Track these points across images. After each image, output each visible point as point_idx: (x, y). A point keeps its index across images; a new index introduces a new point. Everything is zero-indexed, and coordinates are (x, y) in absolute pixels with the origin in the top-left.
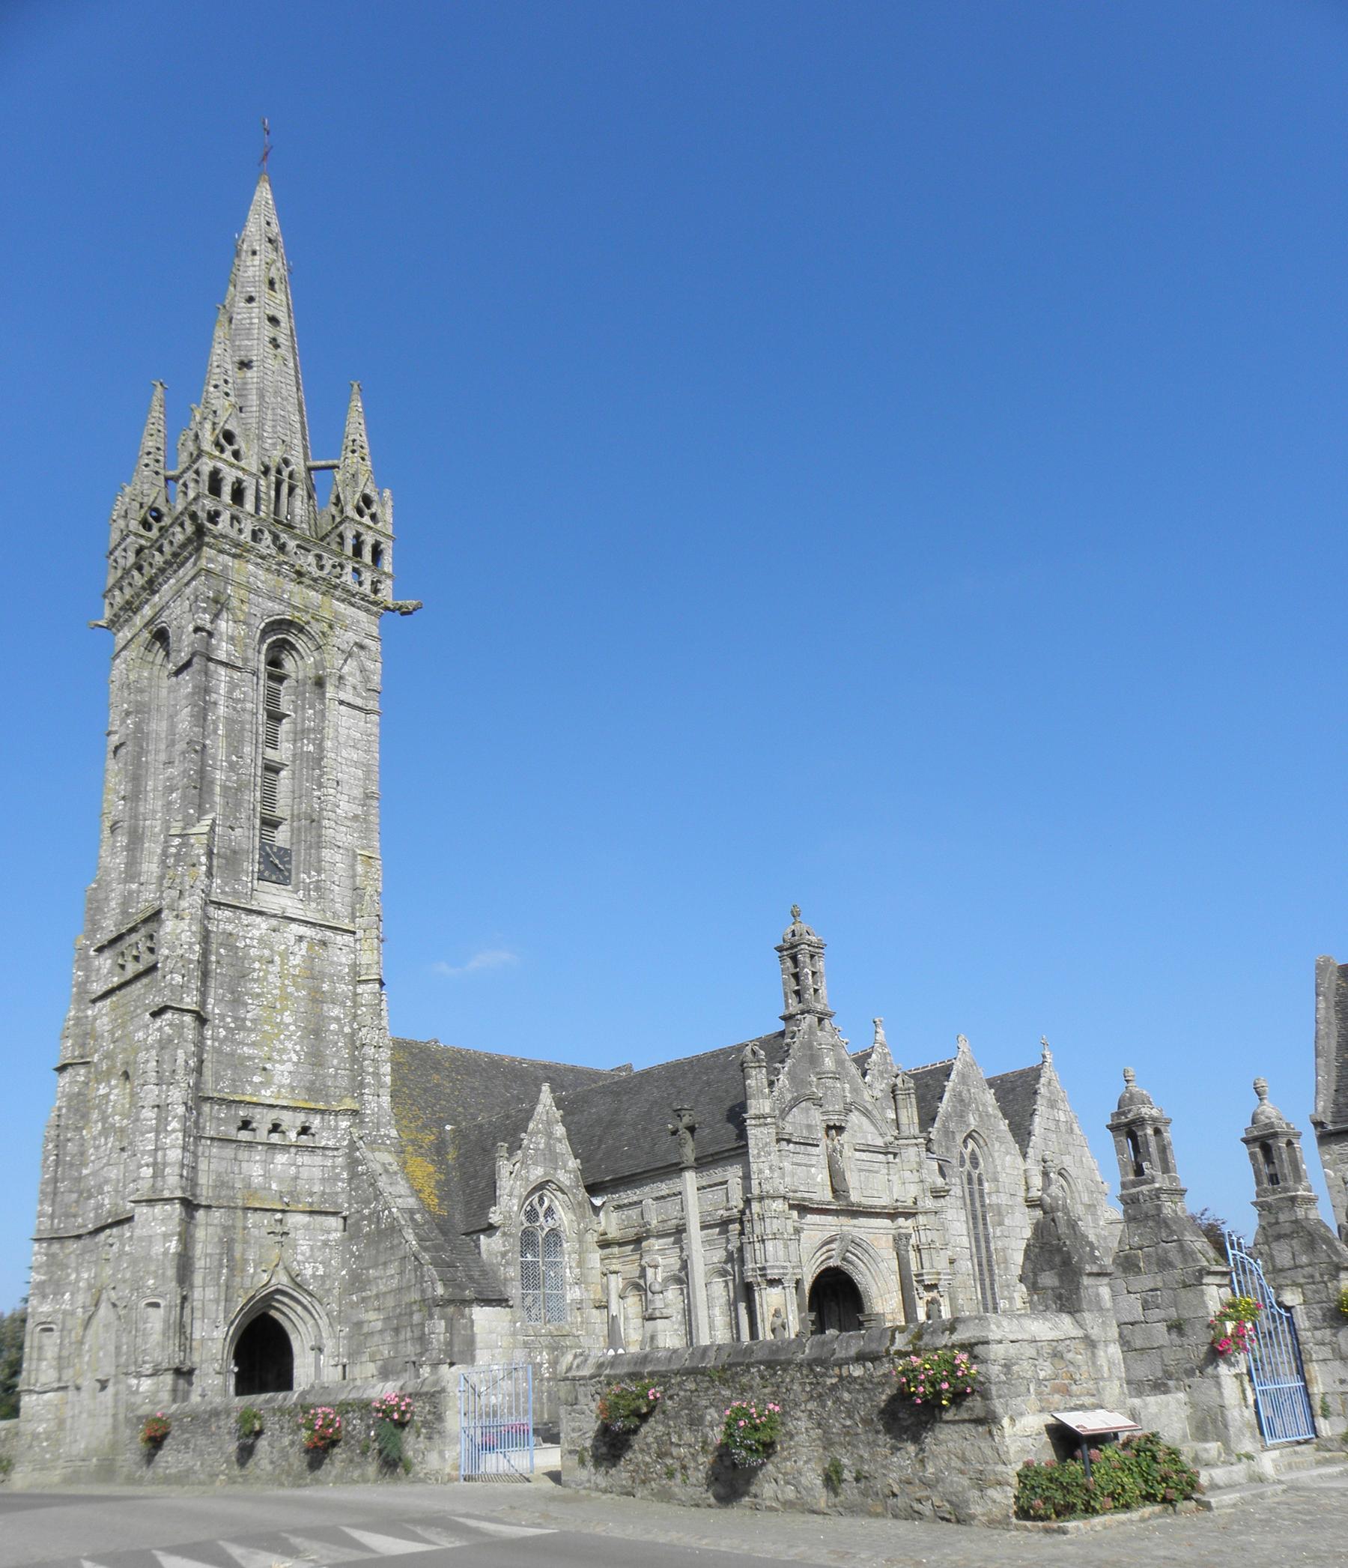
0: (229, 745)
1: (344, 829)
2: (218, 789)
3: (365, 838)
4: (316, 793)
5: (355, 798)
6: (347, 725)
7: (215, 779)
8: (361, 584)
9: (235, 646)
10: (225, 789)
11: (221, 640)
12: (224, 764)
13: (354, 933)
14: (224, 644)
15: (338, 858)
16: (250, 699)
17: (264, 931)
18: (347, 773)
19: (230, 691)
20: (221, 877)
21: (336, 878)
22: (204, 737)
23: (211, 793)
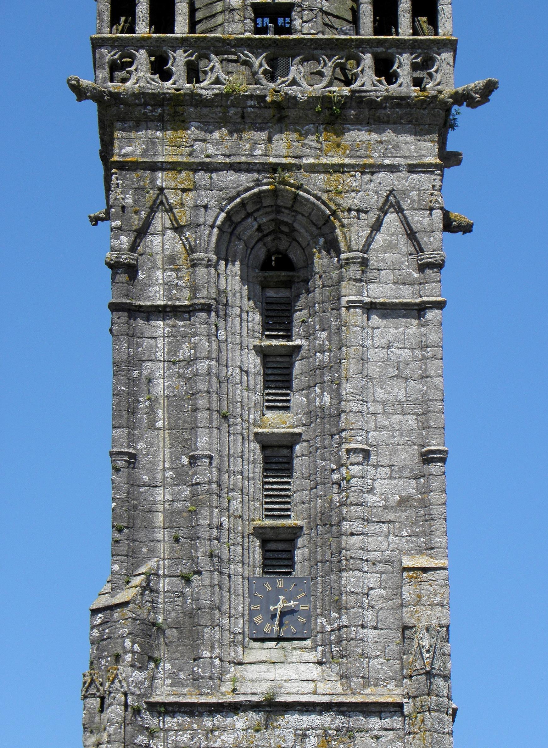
0: (175, 439)
1: (384, 527)
2: (160, 519)
3: (424, 534)
4: (335, 476)
5: (401, 469)
6: (383, 342)
7: (154, 503)
8: (391, 78)
9: (177, 270)
10: (171, 514)
11: (154, 267)
12: (169, 474)
13: (400, 706)
14: (159, 274)
15: (373, 580)
16: (204, 354)
17: (241, 734)
18: (384, 428)
19: (174, 350)
20: (170, 660)
21: (370, 616)
22: (132, 440)
23: (150, 527)
